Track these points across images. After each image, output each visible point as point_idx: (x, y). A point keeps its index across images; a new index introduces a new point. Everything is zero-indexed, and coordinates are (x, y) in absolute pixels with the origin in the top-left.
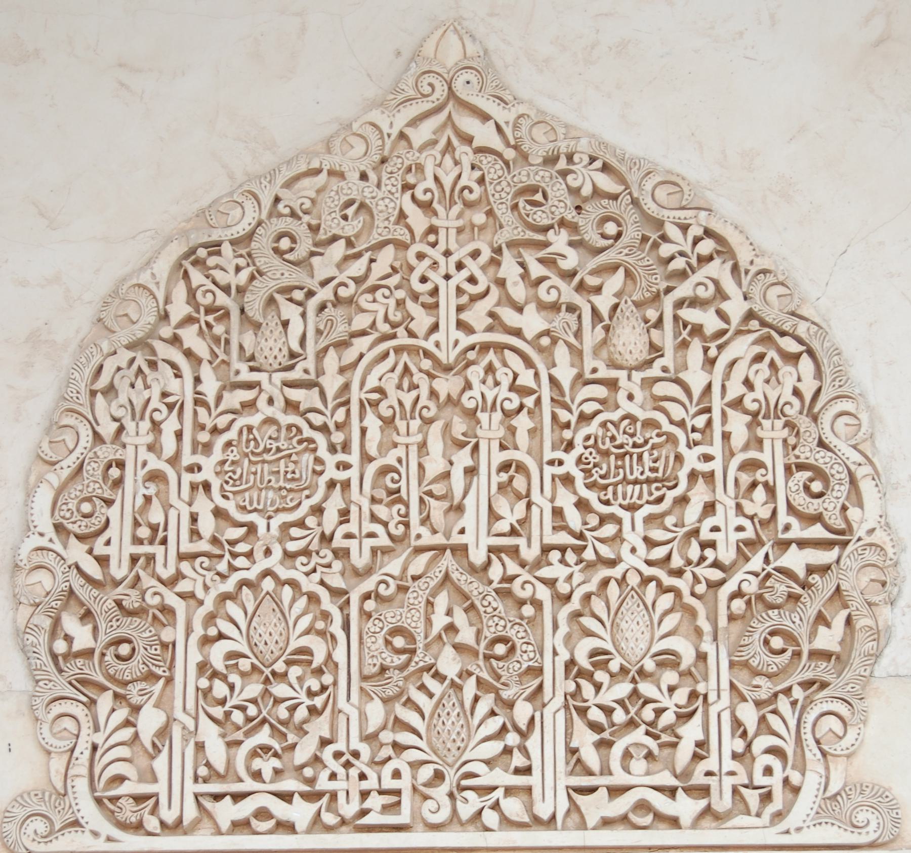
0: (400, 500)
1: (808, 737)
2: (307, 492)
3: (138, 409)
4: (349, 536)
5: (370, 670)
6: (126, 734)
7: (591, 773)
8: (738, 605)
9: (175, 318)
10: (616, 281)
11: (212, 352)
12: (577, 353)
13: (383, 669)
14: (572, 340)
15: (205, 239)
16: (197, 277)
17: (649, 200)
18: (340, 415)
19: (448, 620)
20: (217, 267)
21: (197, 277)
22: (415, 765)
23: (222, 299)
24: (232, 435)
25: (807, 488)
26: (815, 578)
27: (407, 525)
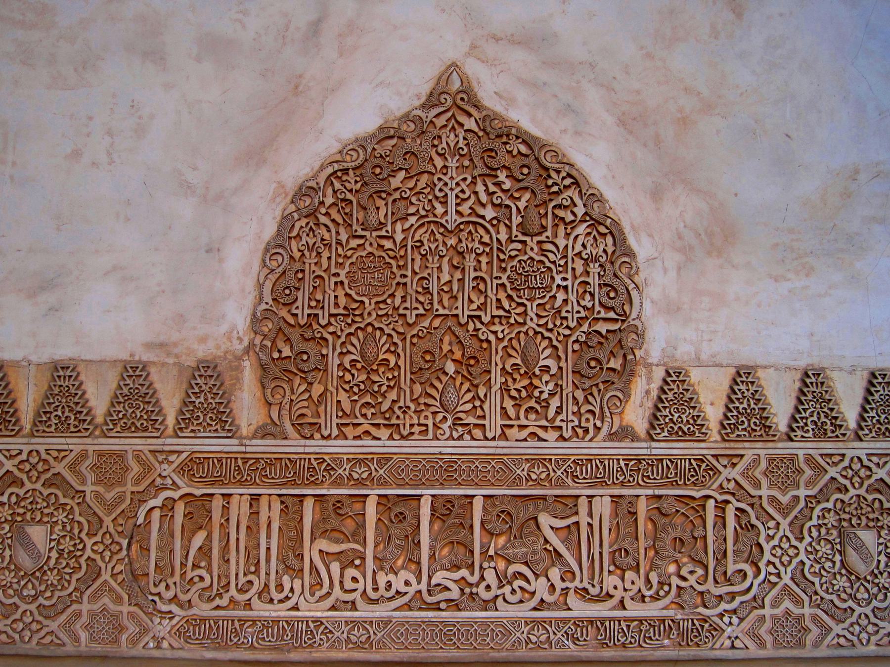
2: (387, 288)
4: (406, 308)
5: (415, 370)
6: (306, 396)
7: (510, 419)
8: (576, 347)
10: (527, 196)
11: (344, 219)
12: (509, 228)
13: (421, 369)
15: (341, 167)
17: (543, 158)
19: (449, 348)
21: (337, 185)
23: (349, 196)
24: (354, 259)
25: (608, 295)
26: (610, 336)
27: (432, 304)
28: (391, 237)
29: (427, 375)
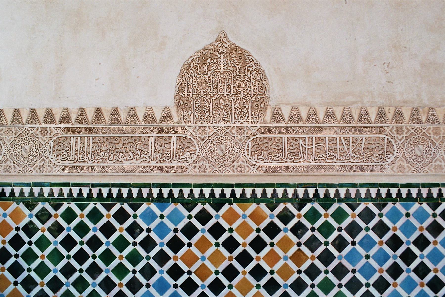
4: (211, 92)
5: (213, 107)
6: (187, 114)
10: (241, 64)
16: (194, 62)
18: (210, 79)
19: (222, 102)
20: (196, 61)
21: (194, 62)
23: (197, 65)
24: (198, 81)
26: (261, 99)
29: (216, 109)
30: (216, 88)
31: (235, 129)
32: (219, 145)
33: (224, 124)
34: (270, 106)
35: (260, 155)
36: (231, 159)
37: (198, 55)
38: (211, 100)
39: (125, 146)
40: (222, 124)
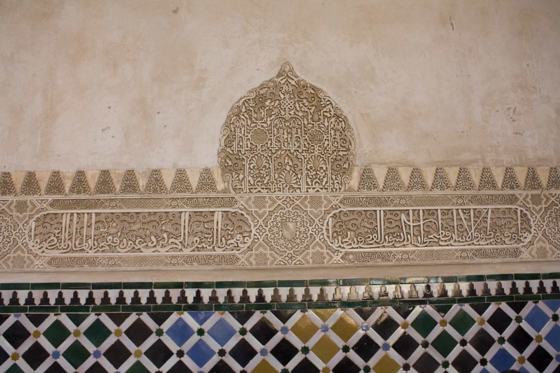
0: (280, 142)
1: (343, 181)
3: (238, 126)
4: (272, 148)
5: (275, 169)
6: (237, 179)
8: (332, 160)
9: (243, 111)
10: (314, 108)
11: (250, 117)
13: (278, 169)
14: (307, 117)
15: (248, 98)
16: (246, 105)
19: (288, 161)
21: (246, 105)
22: (283, 184)
23: (251, 108)
24: (253, 131)
26: (344, 156)
27: (281, 146)
28: (266, 123)
29: (280, 171)
30: (279, 141)
31: (308, 200)
32: (286, 223)
33: (292, 192)
34: (357, 166)
35: (345, 237)
36: (303, 243)
37: (253, 94)
38: (271, 159)
39: (146, 226)
40: (289, 192)
